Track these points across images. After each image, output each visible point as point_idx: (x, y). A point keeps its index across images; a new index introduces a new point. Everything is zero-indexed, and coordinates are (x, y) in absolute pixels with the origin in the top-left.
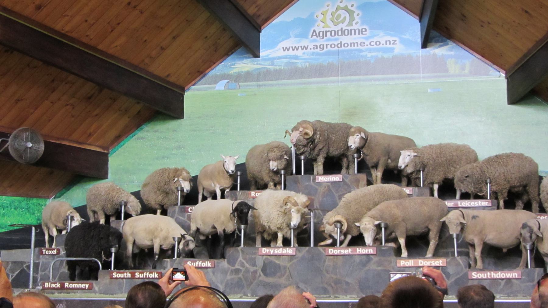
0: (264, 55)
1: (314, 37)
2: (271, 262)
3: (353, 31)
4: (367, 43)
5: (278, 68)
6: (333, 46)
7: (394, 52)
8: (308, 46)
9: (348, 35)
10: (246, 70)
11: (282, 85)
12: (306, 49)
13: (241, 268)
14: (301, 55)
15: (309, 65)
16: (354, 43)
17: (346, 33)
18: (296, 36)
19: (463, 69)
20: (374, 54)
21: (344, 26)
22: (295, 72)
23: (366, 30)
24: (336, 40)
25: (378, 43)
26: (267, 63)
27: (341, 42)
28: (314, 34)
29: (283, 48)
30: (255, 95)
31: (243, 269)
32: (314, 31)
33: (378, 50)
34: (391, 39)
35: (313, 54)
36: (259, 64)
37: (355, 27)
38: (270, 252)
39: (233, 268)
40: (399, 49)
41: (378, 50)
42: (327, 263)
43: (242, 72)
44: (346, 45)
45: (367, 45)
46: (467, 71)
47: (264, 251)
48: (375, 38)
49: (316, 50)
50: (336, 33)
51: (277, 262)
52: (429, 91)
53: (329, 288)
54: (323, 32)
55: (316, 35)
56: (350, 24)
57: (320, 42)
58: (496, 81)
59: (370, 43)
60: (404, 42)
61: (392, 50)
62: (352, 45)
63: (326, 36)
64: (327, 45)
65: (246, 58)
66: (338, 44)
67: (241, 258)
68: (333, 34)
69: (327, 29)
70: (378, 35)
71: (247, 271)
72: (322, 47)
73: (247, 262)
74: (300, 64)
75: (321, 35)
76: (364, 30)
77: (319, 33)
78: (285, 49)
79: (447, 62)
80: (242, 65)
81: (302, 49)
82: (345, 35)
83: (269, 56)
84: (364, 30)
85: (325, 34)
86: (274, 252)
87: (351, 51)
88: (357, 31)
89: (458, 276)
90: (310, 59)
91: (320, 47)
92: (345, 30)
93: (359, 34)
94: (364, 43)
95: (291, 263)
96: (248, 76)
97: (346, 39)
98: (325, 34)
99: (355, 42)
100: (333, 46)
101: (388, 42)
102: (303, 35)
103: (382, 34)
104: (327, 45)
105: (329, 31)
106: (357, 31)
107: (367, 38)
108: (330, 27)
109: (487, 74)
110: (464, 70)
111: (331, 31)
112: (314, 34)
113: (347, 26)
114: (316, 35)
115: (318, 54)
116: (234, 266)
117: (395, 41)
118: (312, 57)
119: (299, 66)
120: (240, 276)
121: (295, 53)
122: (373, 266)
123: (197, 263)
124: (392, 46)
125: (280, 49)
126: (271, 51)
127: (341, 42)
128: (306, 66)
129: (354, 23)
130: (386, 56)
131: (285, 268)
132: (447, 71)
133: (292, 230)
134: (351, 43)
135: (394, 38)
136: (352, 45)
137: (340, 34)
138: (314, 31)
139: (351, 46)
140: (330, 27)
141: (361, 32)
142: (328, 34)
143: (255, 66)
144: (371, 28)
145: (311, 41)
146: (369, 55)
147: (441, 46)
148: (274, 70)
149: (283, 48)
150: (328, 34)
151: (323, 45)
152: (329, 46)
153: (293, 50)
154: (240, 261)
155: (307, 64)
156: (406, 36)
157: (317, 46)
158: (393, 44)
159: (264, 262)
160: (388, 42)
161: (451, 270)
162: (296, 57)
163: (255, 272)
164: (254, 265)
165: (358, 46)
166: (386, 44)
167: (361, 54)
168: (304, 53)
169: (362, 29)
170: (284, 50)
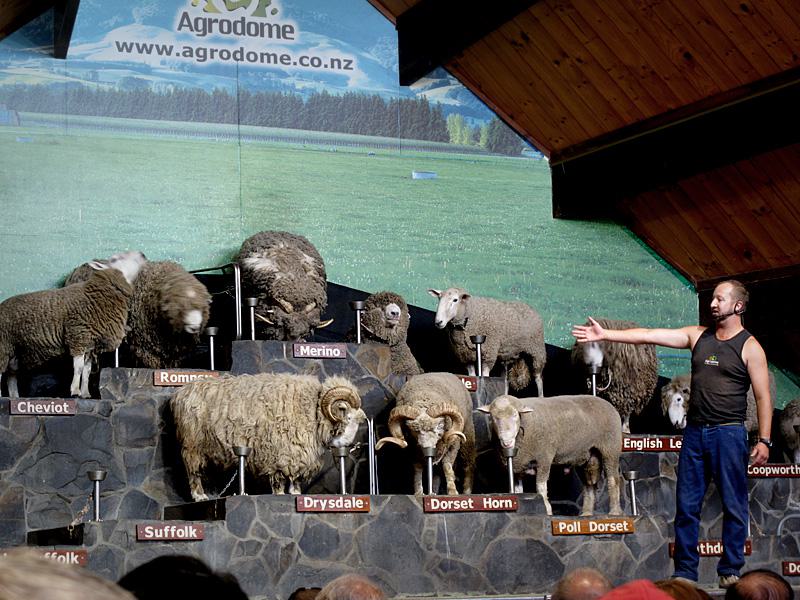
0: (76, 54)
1: (186, 30)
2: (321, 526)
3: (266, 28)
4: (295, 58)
5: (106, 87)
6: (225, 55)
7: (347, 85)
8: (171, 47)
9: (256, 35)
10: (33, 82)
11: (117, 127)
12: (169, 53)
13: (258, 540)
14: (159, 65)
15: (176, 89)
16: (269, 56)
17: (253, 31)
18: (148, 21)
19: (476, 137)
20: (308, 84)
21: (248, 13)
22: (137, 102)
23: (292, 31)
24: (232, 42)
25: (316, 62)
26: (82, 72)
27: (242, 49)
28: (186, 22)
29: (117, 43)
30: (55, 143)
31: (265, 542)
32: (185, 15)
33: (318, 78)
34: (343, 57)
35: (182, 66)
36: (66, 74)
37: (270, 19)
38: (319, 504)
39: (242, 540)
40: (357, 81)
41: (318, 78)
42: (425, 528)
43: (25, 86)
44: (252, 57)
45: (295, 64)
46: (482, 143)
47: (309, 502)
48: (311, 49)
49: (188, 60)
50: (232, 27)
51: (332, 525)
52: (415, 175)
53: (434, 578)
54: (204, 20)
55: (190, 25)
56: (260, 12)
57: (198, 42)
58: (534, 171)
59: (301, 59)
60: (365, 65)
61: (344, 80)
62: (265, 57)
63: (210, 31)
64: (212, 51)
65: (34, 55)
66: (235, 53)
67: (257, 519)
68: (225, 29)
69: (213, 16)
70: (317, 44)
71: (273, 544)
72: (201, 53)
73: (271, 527)
74: (156, 85)
75: (200, 27)
76: (288, 29)
77: (196, 20)
78: (123, 47)
79: (448, 120)
80: (23, 70)
81: (160, 53)
82: (250, 34)
83: (87, 59)
84: (288, 29)
85: (208, 25)
86: (327, 504)
87: (265, 71)
88: (274, 29)
89: (653, 551)
90: (178, 78)
91: (198, 55)
92: (250, 24)
93: (279, 37)
94: (289, 58)
95: (360, 528)
96: (36, 99)
97: (253, 44)
98: (208, 25)
99: (270, 53)
100: (225, 55)
101: (336, 63)
102: (161, 21)
103: (324, 42)
104: (212, 51)
105: (216, 21)
106: (274, 29)
107: (295, 48)
108: (217, 11)
109: (516, 153)
110: (479, 141)
111: (222, 21)
112: (186, 22)
113: (254, 15)
114: (190, 25)
115: (193, 69)
116: (244, 536)
117: (350, 62)
118: (181, 72)
119: (155, 90)
120: (259, 555)
121: (144, 58)
122: (508, 534)
123: (166, 529)
124: (343, 72)
125: (110, 45)
126: (93, 45)
127: (242, 49)
128: (169, 92)
129: (268, 10)
130: (332, 92)
131: (348, 537)
132: (446, 138)
133: (242, 458)
134: (262, 55)
135: (349, 57)
136: (265, 57)
137: (239, 30)
138: (185, 15)
139: (262, 61)
140: (217, 11)
141: (282, 32)
142: (216, 26)
143: (52, 76)
144: (304, 28)
145: (179, 38)
146: (299, 86)
147: (435, 86)
148: (98, 91)
149: (117, 43)
150: (216, 26)
151: (205, 50)
152: (216, 54)
153: (140, 51)
154: (257, 524)
155: (171, 88)
156: (371, 56)
157: (191, 50)
158: (346, 68)
159: (306, 527)
160: (336, 63)
161: (641, 537)
162: (147, 70)
163: (291, 547)
164: (287, 532)
165: (276, 62)
166: (333, 67)
167: (283, 81)
168: (163, 63)
169: (284, 27)
170: (121, 50)
